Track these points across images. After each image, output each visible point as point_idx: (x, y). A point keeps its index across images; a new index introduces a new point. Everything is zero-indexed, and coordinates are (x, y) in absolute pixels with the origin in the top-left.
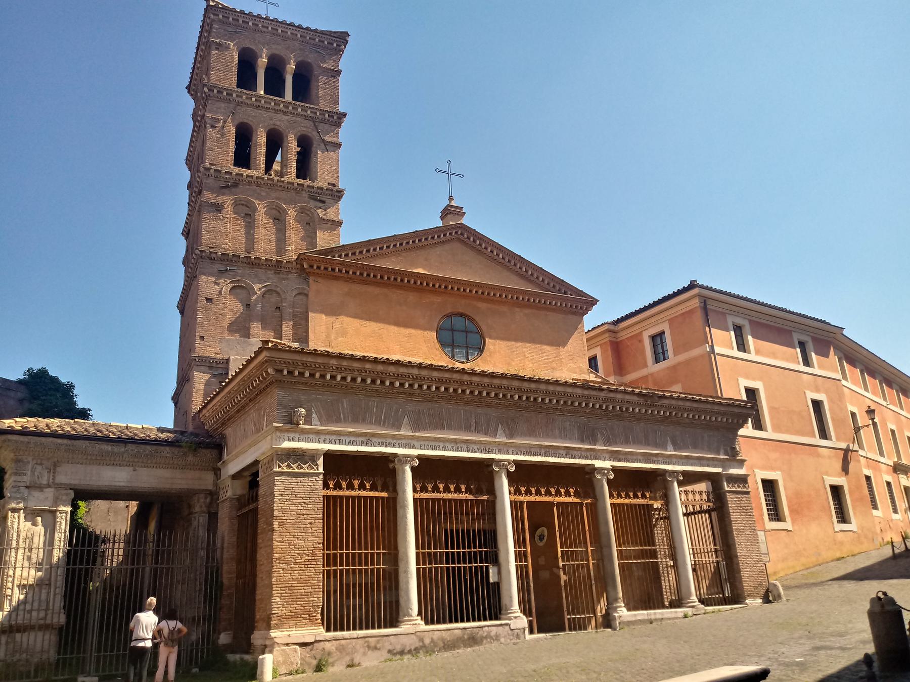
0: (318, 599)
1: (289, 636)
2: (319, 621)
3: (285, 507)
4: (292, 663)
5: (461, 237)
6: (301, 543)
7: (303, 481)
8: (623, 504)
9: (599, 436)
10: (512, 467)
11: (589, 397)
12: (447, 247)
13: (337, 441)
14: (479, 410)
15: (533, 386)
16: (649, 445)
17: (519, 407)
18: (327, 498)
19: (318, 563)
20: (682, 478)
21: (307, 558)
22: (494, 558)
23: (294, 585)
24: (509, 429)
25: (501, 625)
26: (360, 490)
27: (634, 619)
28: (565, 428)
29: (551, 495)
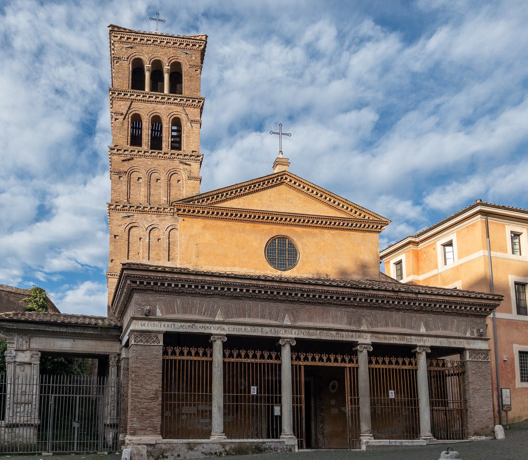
0: (157, 421)
1: (140, 439)
2: (159, 432)
3: (139, 365)
4: (142, 455)
6: (148, 387)
7: (150, 350)
8: (379, 369)
10: (293, 342)
11: (356, 295)
13: (173, 326)
15: (312, 287)
17: (302, 302)
18: (163, 360)
19: (159, 399)
20: (430, 351)
21: (152, 396)
22: (279, 401)
23: (143, 411)
24: (293, 317)
25: (279, 442)
26: (188, 356)
27: (378, 444)
28: (337, 316)
29: (323, 361)
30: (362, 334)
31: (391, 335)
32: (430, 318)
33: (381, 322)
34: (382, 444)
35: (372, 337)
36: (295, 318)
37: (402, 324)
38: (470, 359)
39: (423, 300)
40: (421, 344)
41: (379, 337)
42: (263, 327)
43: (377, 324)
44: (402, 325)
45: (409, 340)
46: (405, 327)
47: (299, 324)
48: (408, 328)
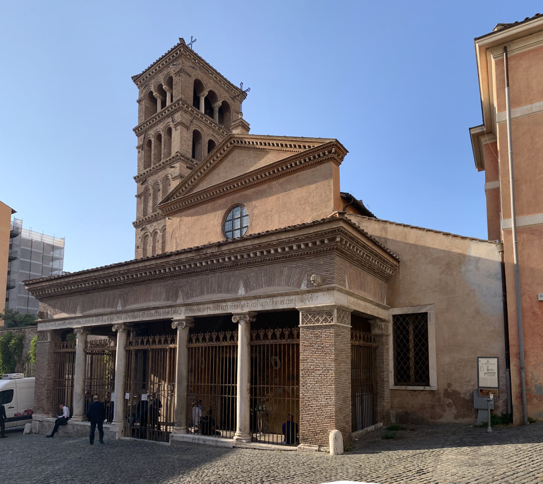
5: (235, 144)
12: (230, 158)
30: (177, 308)
31: (206, 305)
32: (252, 273)
33: (196, 291)
35: (186, 311)
38: (304, 325)
40: (239, 311)
41: (193, 309)
43: (193, 294)
45: (225, 308)
46: (221, 292)
48: (225, 293)
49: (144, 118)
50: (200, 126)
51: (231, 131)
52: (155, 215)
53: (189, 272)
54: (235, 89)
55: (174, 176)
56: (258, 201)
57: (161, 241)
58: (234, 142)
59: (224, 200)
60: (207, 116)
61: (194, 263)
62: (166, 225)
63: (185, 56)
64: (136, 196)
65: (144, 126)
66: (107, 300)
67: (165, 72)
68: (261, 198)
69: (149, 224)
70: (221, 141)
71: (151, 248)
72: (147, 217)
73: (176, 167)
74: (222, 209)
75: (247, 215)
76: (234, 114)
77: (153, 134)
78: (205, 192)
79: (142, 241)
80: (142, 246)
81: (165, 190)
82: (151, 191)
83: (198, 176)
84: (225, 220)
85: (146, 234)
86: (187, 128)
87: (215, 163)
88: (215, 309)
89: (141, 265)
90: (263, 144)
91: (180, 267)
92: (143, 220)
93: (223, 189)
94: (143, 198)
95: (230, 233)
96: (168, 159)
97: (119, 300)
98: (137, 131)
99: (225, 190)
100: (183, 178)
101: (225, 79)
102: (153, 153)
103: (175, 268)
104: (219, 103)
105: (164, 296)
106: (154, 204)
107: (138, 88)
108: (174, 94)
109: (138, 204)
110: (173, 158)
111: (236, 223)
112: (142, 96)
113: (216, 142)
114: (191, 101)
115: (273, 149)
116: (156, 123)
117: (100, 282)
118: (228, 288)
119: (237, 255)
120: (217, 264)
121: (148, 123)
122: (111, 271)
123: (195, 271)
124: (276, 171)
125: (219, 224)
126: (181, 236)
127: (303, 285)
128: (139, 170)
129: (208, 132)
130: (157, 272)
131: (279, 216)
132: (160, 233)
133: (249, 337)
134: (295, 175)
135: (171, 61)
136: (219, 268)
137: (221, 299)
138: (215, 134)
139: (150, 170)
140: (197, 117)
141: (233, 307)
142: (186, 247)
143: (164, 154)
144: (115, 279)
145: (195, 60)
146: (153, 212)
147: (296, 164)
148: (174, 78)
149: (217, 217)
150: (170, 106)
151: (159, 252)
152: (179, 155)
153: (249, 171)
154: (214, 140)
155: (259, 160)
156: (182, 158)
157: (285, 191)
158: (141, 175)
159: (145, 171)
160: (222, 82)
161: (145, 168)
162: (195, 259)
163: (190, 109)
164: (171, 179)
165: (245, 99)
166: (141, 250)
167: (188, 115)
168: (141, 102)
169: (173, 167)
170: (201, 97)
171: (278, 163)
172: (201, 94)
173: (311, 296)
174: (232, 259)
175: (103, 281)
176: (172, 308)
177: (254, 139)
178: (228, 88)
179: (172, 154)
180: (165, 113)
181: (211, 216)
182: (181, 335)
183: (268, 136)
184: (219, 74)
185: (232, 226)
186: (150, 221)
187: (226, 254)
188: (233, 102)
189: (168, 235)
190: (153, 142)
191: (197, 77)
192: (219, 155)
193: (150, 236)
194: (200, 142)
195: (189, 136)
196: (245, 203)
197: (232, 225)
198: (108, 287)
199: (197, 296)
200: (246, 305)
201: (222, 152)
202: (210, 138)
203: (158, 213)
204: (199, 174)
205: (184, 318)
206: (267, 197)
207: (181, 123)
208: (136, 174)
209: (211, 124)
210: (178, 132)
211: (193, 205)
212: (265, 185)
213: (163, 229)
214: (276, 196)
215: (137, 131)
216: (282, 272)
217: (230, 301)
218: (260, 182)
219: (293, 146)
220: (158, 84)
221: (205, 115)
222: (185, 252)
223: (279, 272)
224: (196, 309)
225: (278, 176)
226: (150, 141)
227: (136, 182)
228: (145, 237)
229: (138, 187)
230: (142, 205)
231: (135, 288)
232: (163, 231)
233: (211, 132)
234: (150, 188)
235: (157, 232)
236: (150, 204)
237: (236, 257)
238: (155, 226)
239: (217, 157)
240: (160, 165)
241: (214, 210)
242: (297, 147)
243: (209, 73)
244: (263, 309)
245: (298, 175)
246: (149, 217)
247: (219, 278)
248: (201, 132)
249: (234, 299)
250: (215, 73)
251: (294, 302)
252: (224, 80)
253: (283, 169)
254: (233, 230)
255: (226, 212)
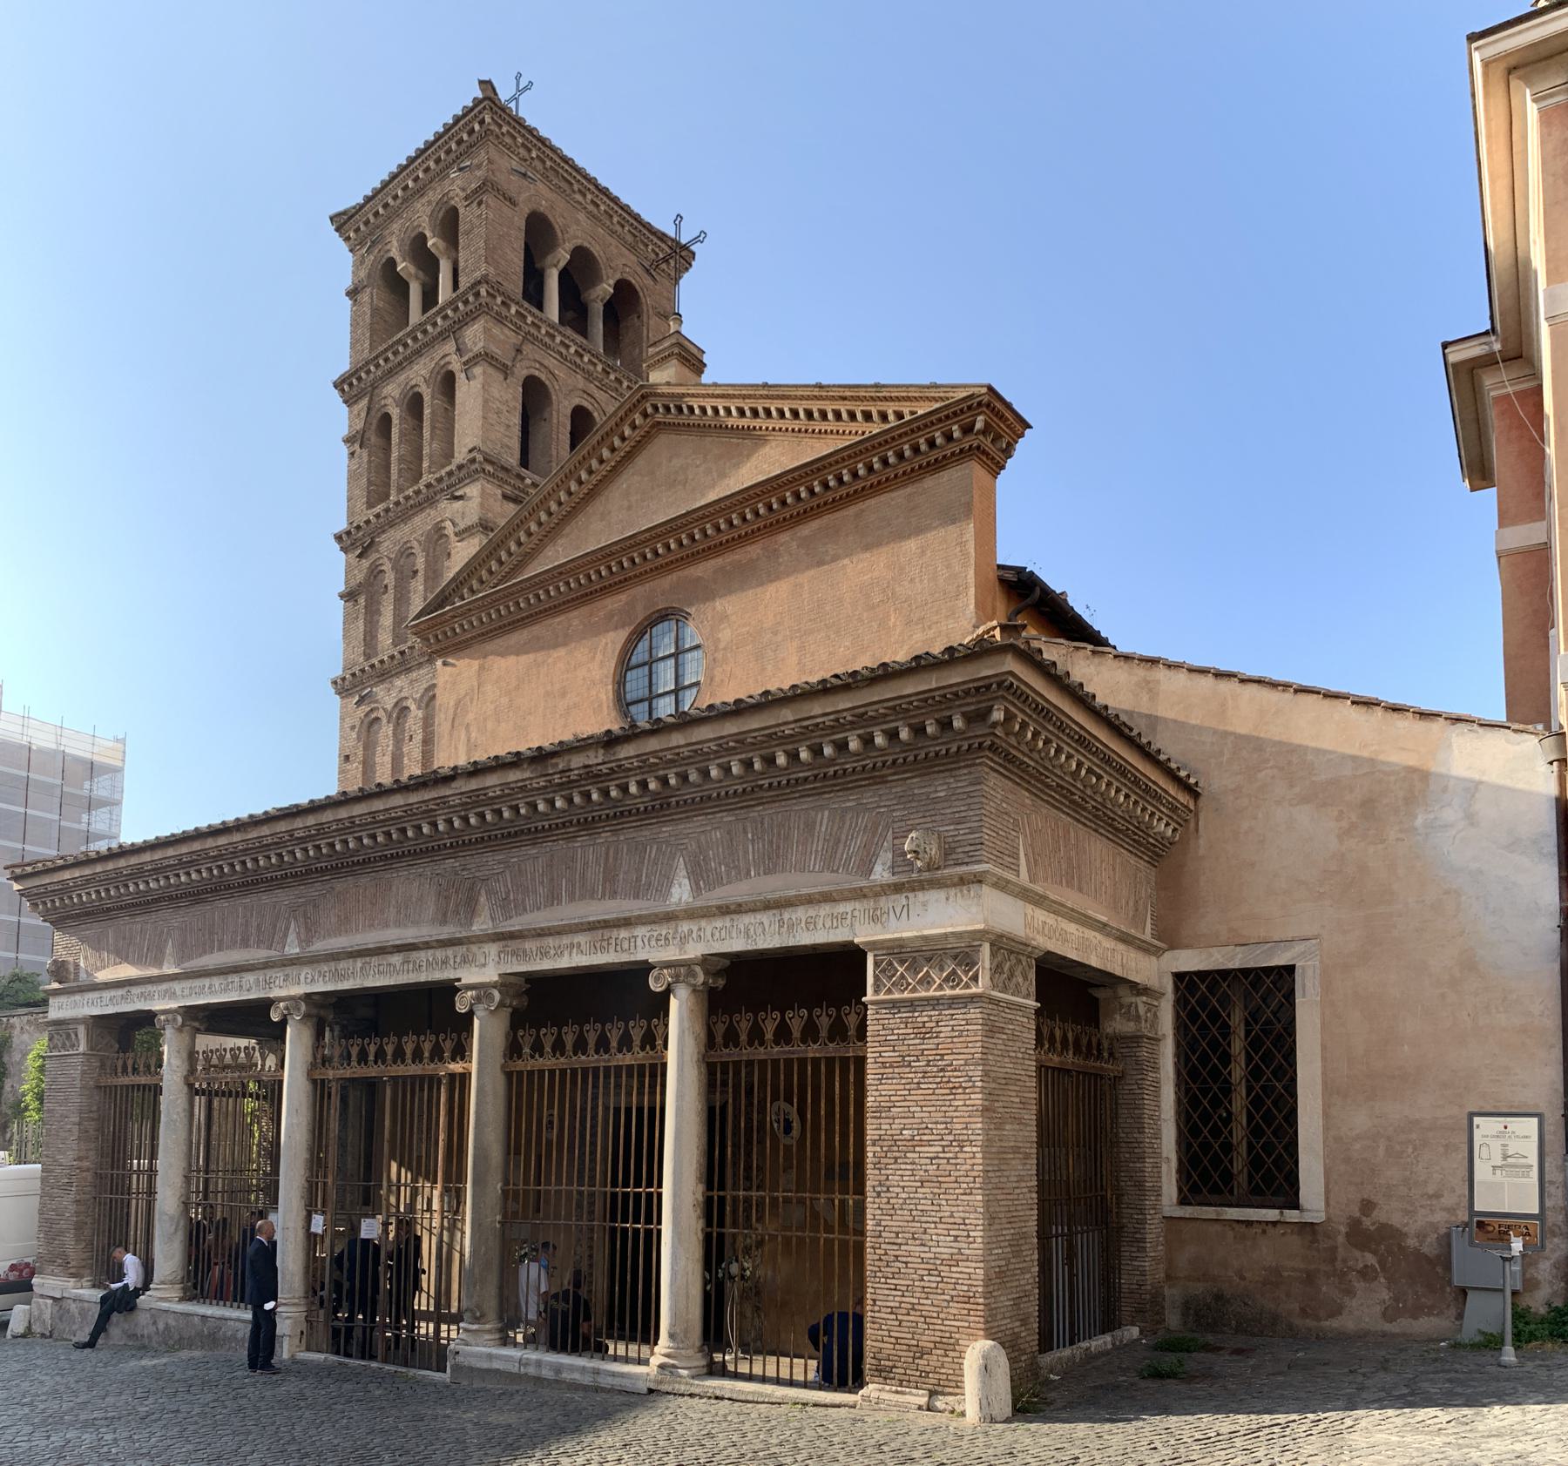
5: (659, 417)
9: (482, 899)
12: (641, 461)
14: (266, 899)
16: (614, 895)
30: (474, 948)
31: (564, 937)
32: (709, 831)
33: (535, 892)
34: (496, 1365)
36: (310, 932)
37: (605, 881)
38: (882, 997)
39: (645, 765)
40: (671, 954)
41: (524, 951)
42: (244, 975)
43: (523, 901)
44: (604, 888)
45: (626, 946)
47: (319, 946)
49: (367, 345)
50: (546, 362)
51: (645, 375)
52: (402, 653)
53: (512, 830)
54: (655, 240)
55: (462, 526)
56: (733, 598)
57: (418, 738)
58: (656, 408)
59: (623, 597)
60: (569, 332)
61: (527, 803)
62: (434, 686)
63: (497, 137)
64: (342, 596)
65: (368, 372)
66: (255, 924)
67: (433, 195)
68: (742, 589)
69: (382, 682)
70: (610, 409)
71: (388, 759)
72: (375, 661)
73: (470, 498)
74: (616, 628)
75: (697, 647)
76: (654, 321)
77: (396, 394)
78: (561, 573)
79: (359, 739)
80: (360, 752)
81: (433, 573)
82: (389, 578)
83: (540, 524)
84: (625, 665)
85: (373, 716)
86: (505, 371)
87: (595, 479)
88: (595, 948)
89: (359, 809)
90: (748, 413)
91: (482, 816)
92: (363, 671)
93: (621, 563)
94: (362, 600)
95: (640, 705)
96: (443, 472)
97: (289, 923)
98: (346, 387)
99: (625, 564)
100: (492, 530)
101: (626, 208)
102: (395, 455)
103: (465, 819)
104: (606, 288)
105: (430, 908)
106: (399, 619)
107: (351, 251)
108: (461, 264)
109: (348, 620)
110: (460, 467)
111: (662, 674)
112: (363, 274)
113: (596, 414)
114: (515, 286)
115: (780, 429)
116: (405, 359)
117: (232, 866)
118: (639, 879)
119: (666, 772)
120: (601, 804)
121: (381, 362)
122: (265, 830)
123: (529, 829)
124: (789, 500)
125: (607, 677)
126: (485, 720)
127: (878, 868)
128: (351, 512)
129: (569, 381)
130: (410, 834)
131: (801, 648)
132: (416, 713)
133: (703, 1035)
134: (852, 511)
135: (453, 156)
136: (607, 815)
137: (614, 916)
138: (592, 389)
139: (387, 510)
140: (536, 333)
141: (653, 943)
142: (501, 749)
143: (431, 456)
144: (280, 856)
145: (529, 151)
146: (395, 645)
147: (855, 475)
148: (461, 211)
149: (599, 656)
150: (451, 304)
151: (413, 768)
152: (479, 457)
153: (703, 503)
154: (590, 408)
155: (737, 466)
156: (489, 468)
157: (821, 563)
158: (358, 527)
159: (370, 514)
160: (615, 219)
161: (370, 505)
162: (532, 790)
163: (513, 311)
164: (452, 536)
165: (687, 269)
166: (355, 767)
167: (506, 331)
168: (359, 297)
169: (460, 498)
170: (548, 272)
171: (796, 474)
172: (549, 259)
173: (905, 903)
174: (652, 786)
175: (244, 863)
176: (456, 948)
177: (718, 396)
178: (635, 236)
179: (456, 455)
180: (435, 324)
181: (581, 652)
182: (486, 1033)
183: (765, 385)
184: (605, 192)
185: (647, 684)
186: (384, 674)
187: (630, 770)
188: (649, 282)
189: (442, 716)
190: (395, 421)
191: (535, 206)
192: (606, 453)
193: (384, 720)
194: (546, 415)
195: (510, 396)
196: (691, 605)
197: (647, 679)
198: (258, 883)
199: (539, 909)
200: (694, 935)
201: (617, 442)
202: (577, 401)
203: (412, 648)
204: (544, 517)
205: (496, 978)
206: (762, 584)
207: (486, 357)
208: (342, 525)
209: (581, 356)
210: (476, 384)
211: (523, 619)
212: (754, 546)
213: (426, 699)
214: (792, 579)
215: (346, 387)
216: (810, 827)
217: (644, 924)
218: (740, 536)
219: (845, 416)
220: (413, 235)
221: (562, 329)
222: (499, 765)
223: (802, 827)
224: (534, 949)
225: (798, 514)
226: (386, 419)
227: (342, 549)
228: (371, 723)
229: (348, 565)
230: (361, 623)
231: (339, 885)
232: (427, 705)
233: (580, 381)
234: (387, 567)
235: (407, 708)
236: (387, 619)
237: (664, 781)
238: (402, 688)
239: (601, 461)
240: (418, 492)
241: (594, 630)
242: (859, 416)
243: (574, 191)
244: (750, 948)
245: (863, 511)
246: (382, 662)
247: (608, 849)
248: (547, 382)
249: (656, 915)
250: (592, 187)
251: (848, 921)
252: (620, 211)
253: (811, 492)
254: (651, 698)
255: (629, 640)
